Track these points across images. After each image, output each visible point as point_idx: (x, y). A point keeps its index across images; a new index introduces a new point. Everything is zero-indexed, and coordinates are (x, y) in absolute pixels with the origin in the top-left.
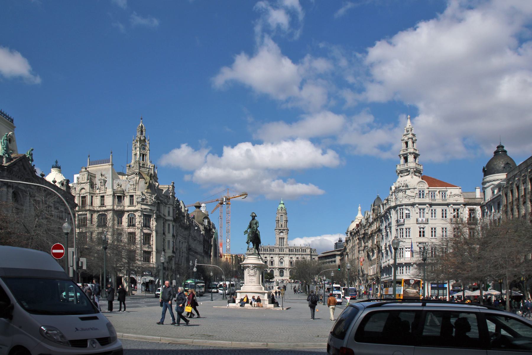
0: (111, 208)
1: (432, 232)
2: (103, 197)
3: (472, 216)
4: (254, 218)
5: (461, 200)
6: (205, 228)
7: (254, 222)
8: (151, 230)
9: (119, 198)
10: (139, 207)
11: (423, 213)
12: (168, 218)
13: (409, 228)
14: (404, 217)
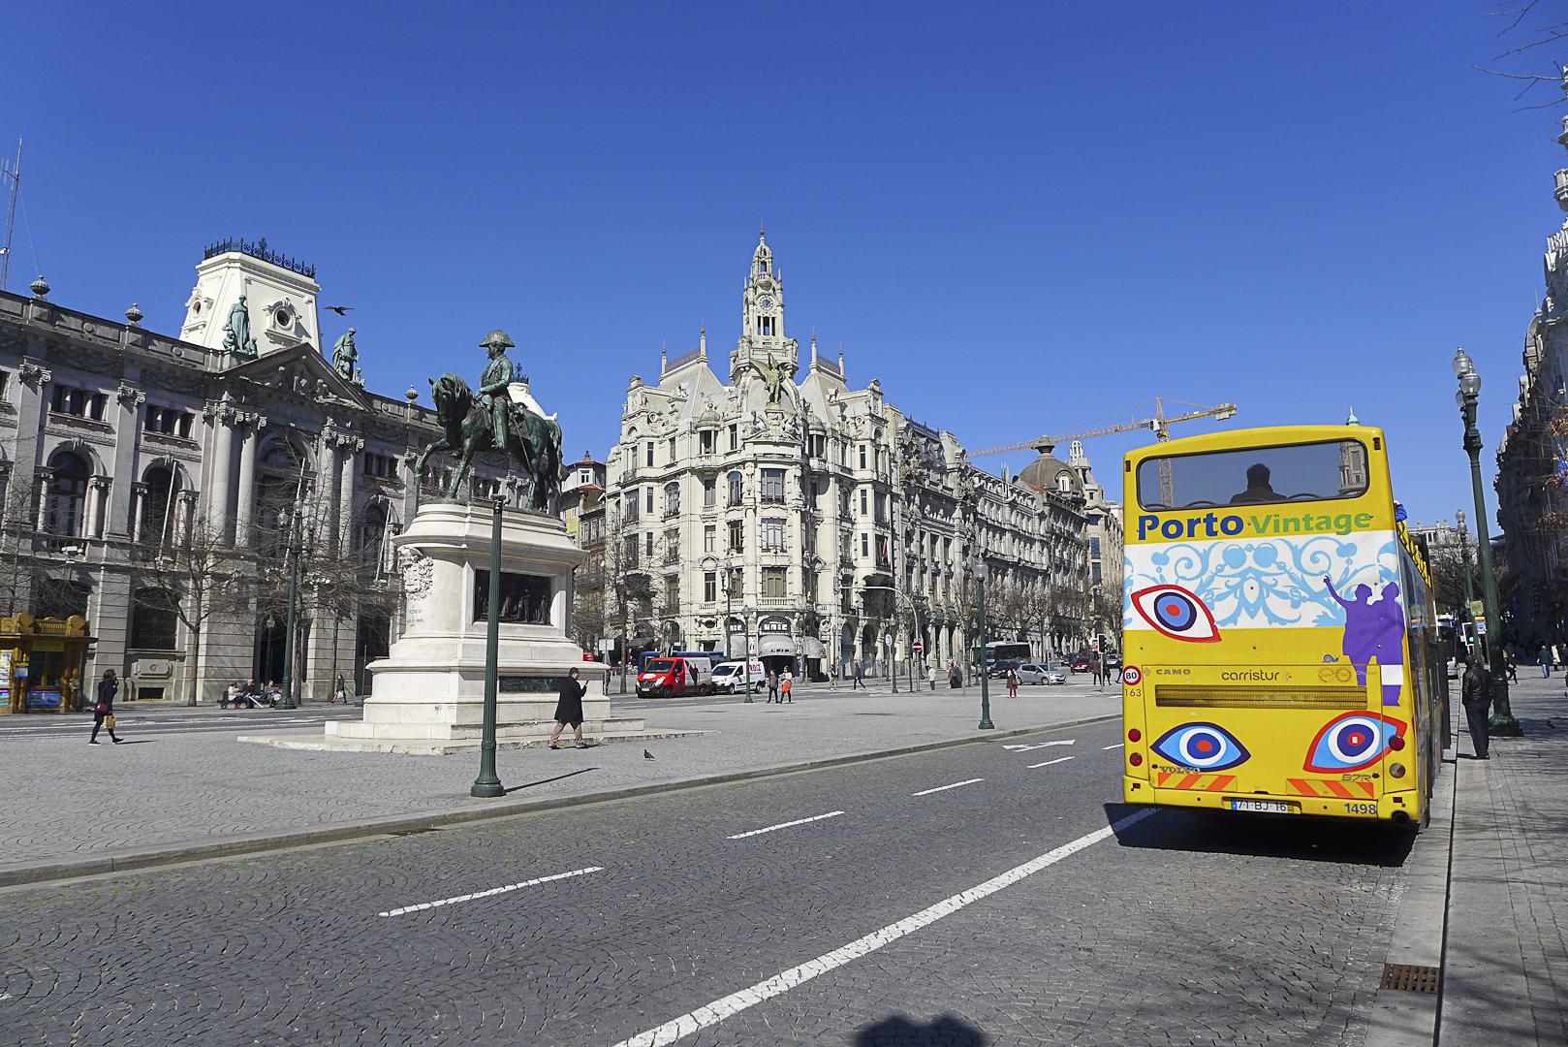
2: (672, 440)
10: (751, 451)
12: (858, 475)
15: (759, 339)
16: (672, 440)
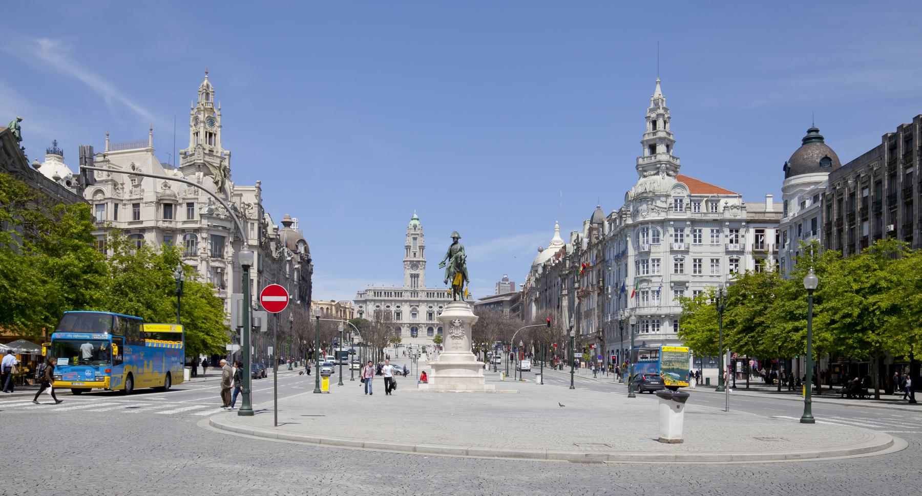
0: (152, 224)
1: (695, 266)
2: (136, 205)
3: (760, 240)
4: (456, 240)
5: (743, 215)
6: (301, 258)
7: (458, 246)
8: (224, 263)
9: (168, 208)
10: (205, 223)
11: (682, 236)
13: (658, 260)
14: (651, 242)
15: (207, 147)
16: (136, 205)
